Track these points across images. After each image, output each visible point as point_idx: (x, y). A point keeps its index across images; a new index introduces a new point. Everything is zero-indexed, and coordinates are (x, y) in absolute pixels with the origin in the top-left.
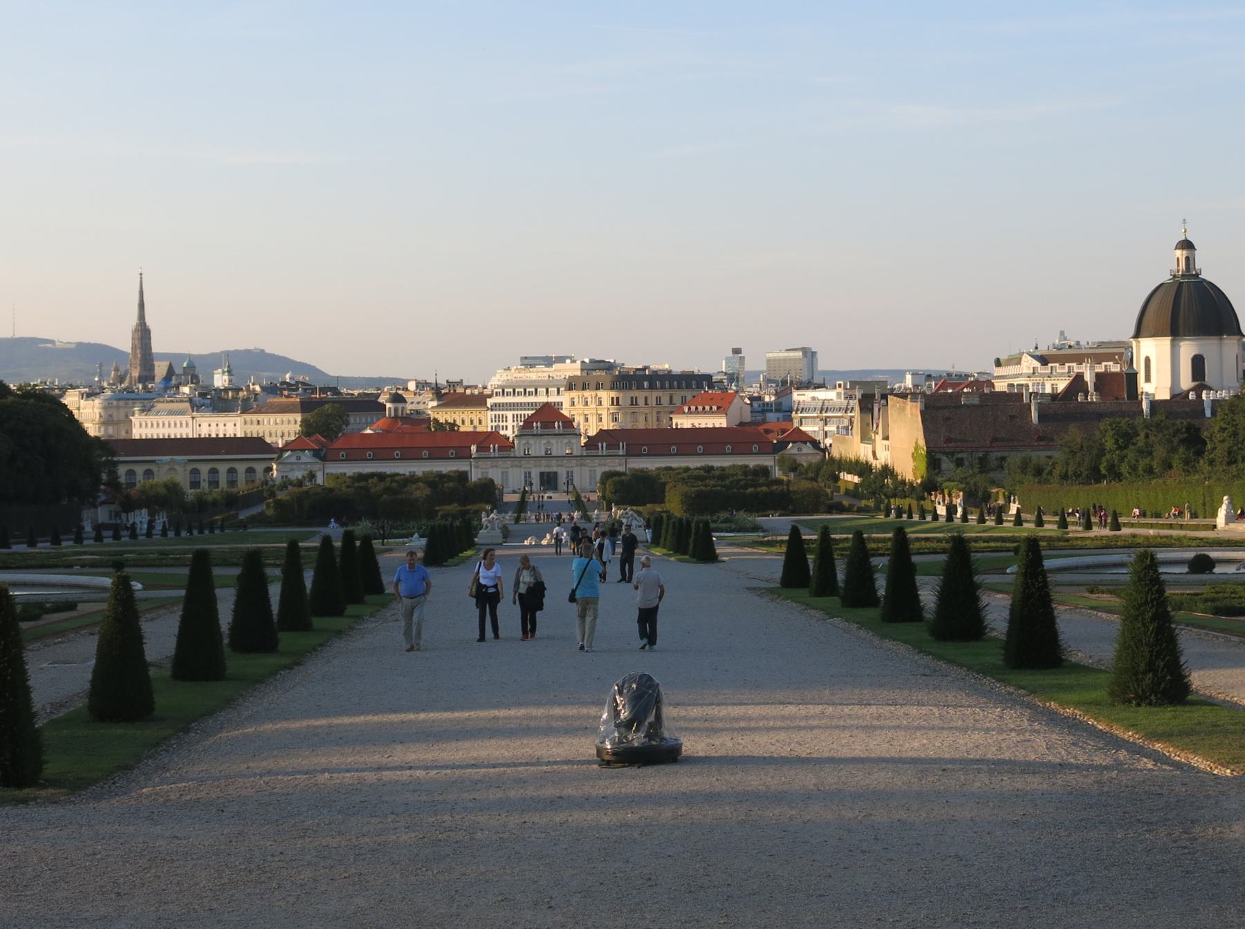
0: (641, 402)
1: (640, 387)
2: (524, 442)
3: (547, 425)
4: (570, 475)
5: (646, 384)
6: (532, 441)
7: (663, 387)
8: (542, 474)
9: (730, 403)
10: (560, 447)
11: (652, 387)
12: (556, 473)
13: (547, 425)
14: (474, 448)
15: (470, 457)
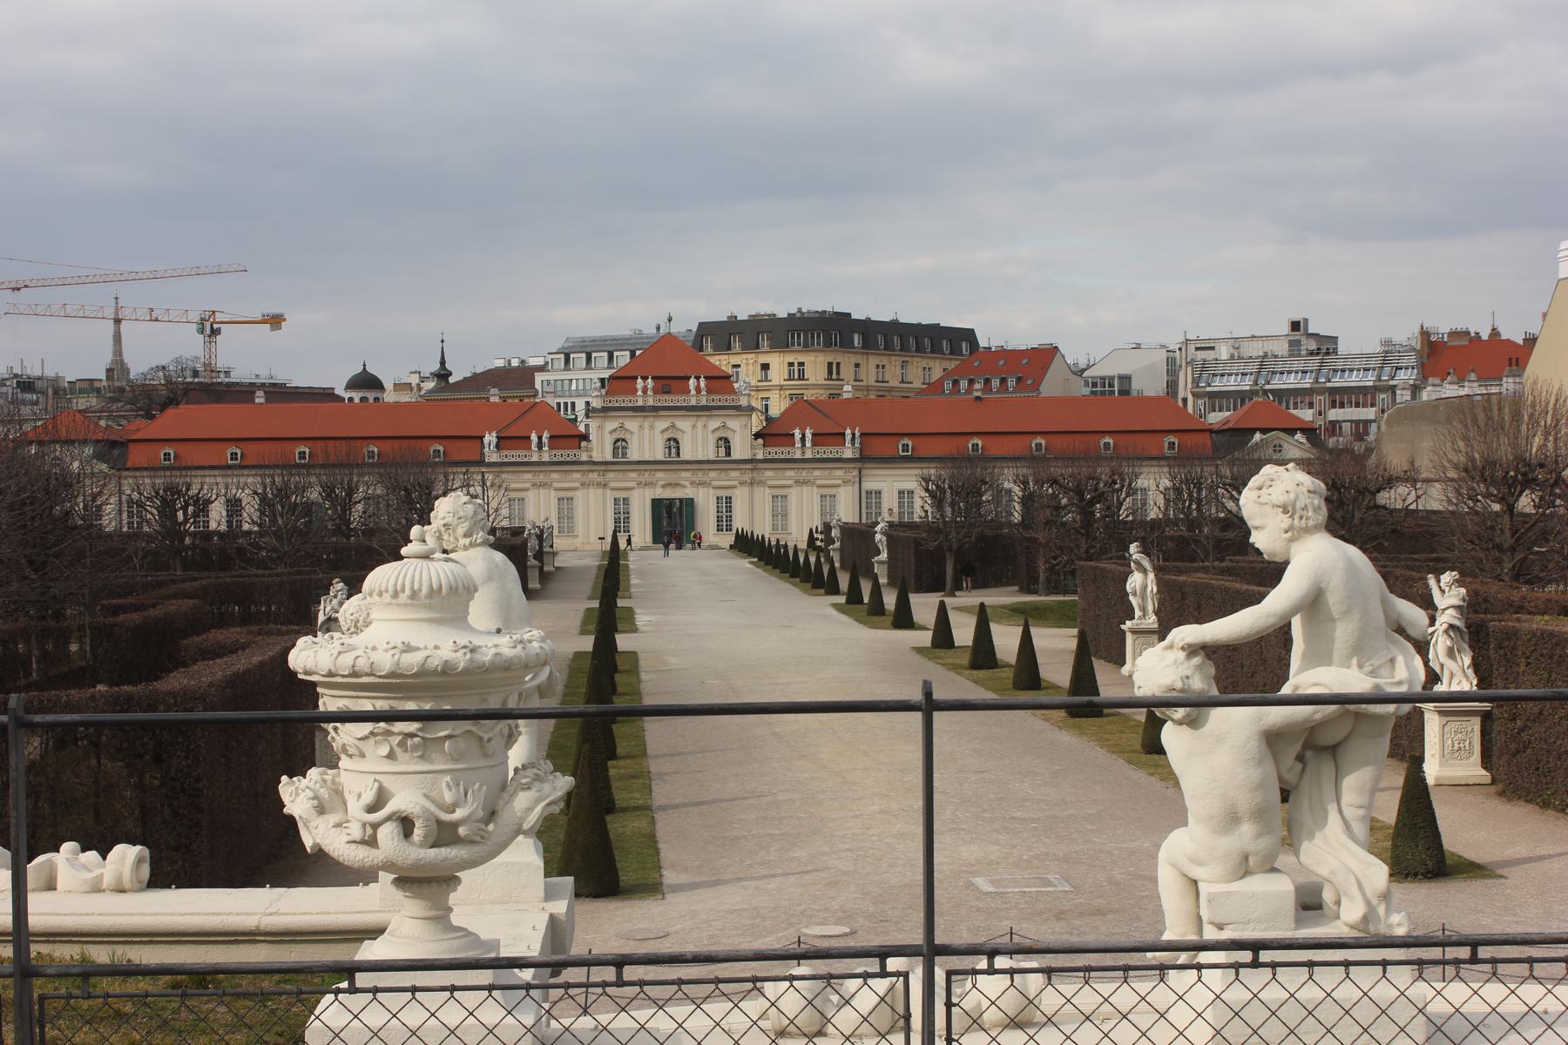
0: (847, 372)
1: (846, 345)
2: (611, 425)
3: (669, 383)
4: (725, 506)
5: (856, 338)
6: (632, 425)
7: (888, 347)
8: (656, 503)
9: (1045, 369)
10: (697, 440)
11: (868, 345)
12: (690, 503)
13: (669, 383)
14: (490, 438)
15: (481, 462)
